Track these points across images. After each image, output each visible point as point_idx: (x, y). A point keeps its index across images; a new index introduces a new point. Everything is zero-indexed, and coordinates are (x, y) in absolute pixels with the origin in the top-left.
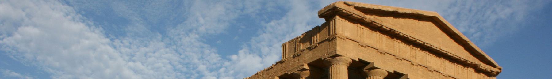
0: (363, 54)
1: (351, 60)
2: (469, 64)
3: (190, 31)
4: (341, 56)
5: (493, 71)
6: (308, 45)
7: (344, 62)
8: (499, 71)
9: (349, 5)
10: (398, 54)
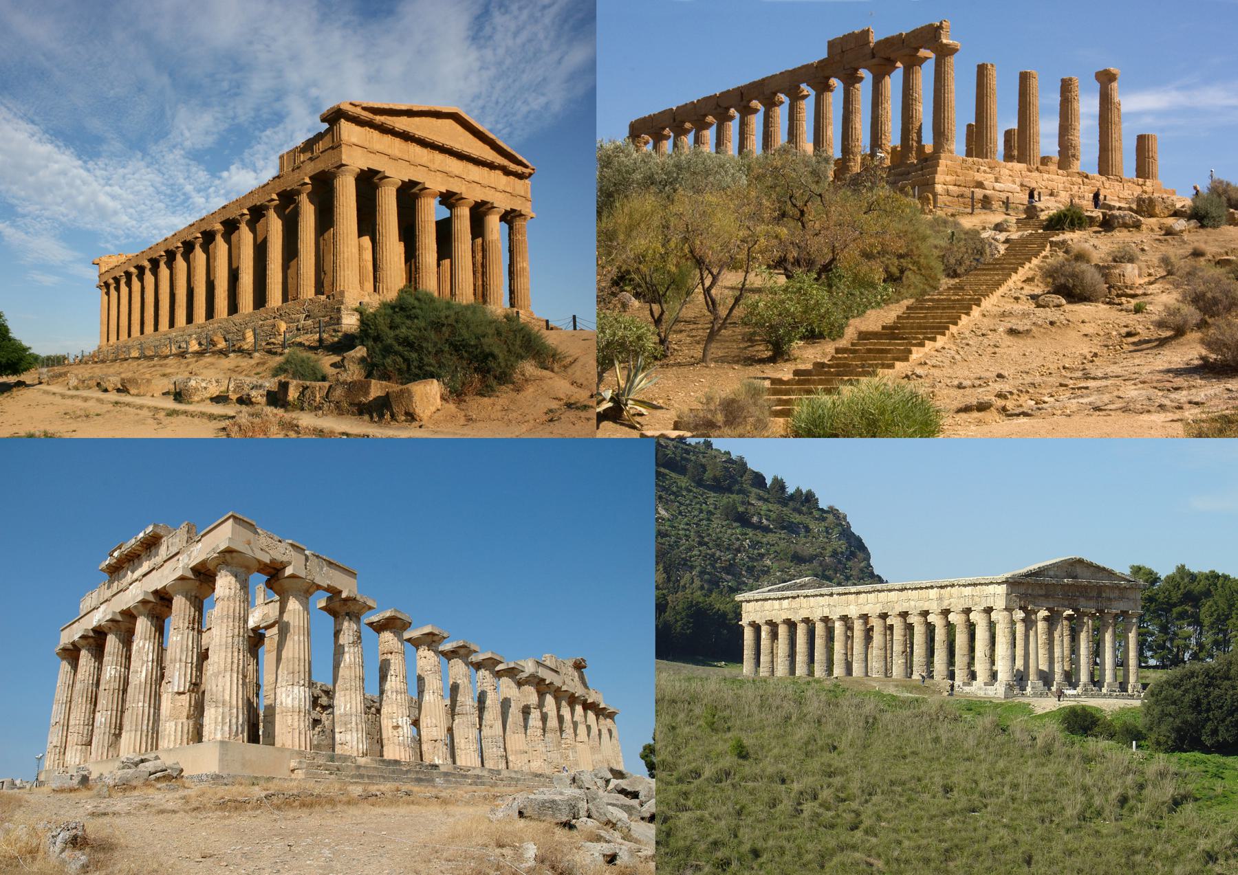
3: (174, 147)
6: (309, 155)
9: (355, 106)
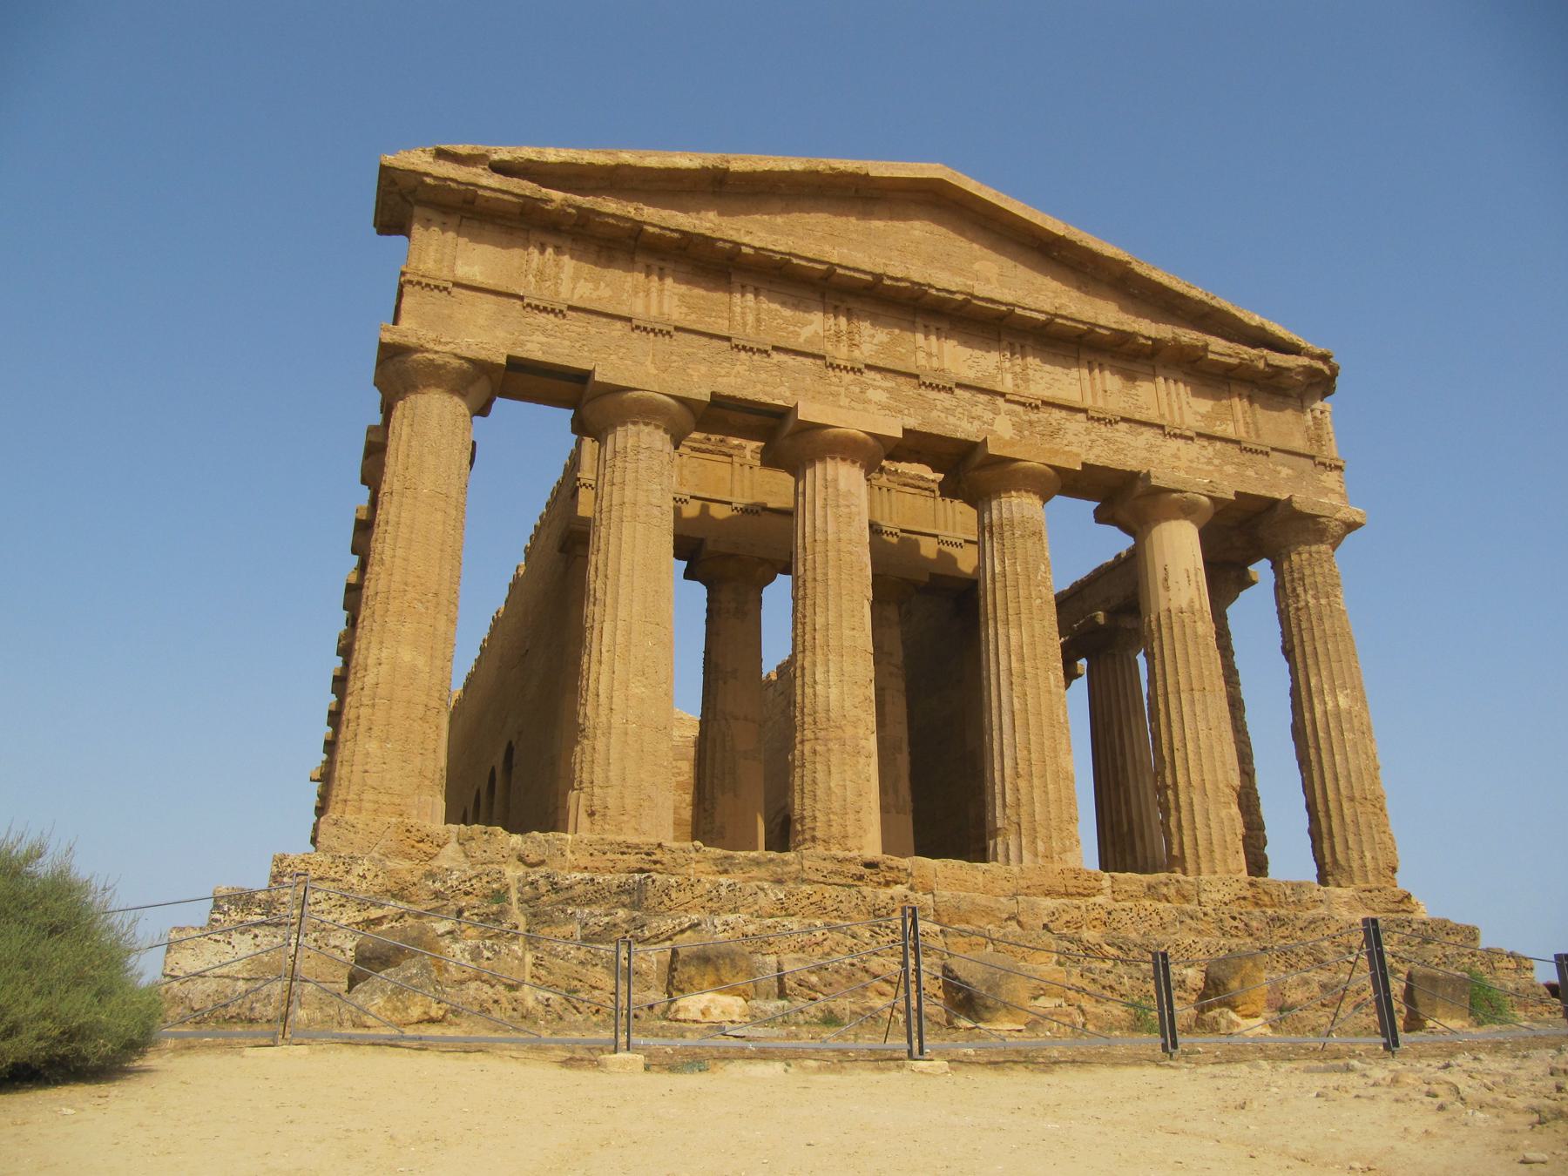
0: (543, 339)
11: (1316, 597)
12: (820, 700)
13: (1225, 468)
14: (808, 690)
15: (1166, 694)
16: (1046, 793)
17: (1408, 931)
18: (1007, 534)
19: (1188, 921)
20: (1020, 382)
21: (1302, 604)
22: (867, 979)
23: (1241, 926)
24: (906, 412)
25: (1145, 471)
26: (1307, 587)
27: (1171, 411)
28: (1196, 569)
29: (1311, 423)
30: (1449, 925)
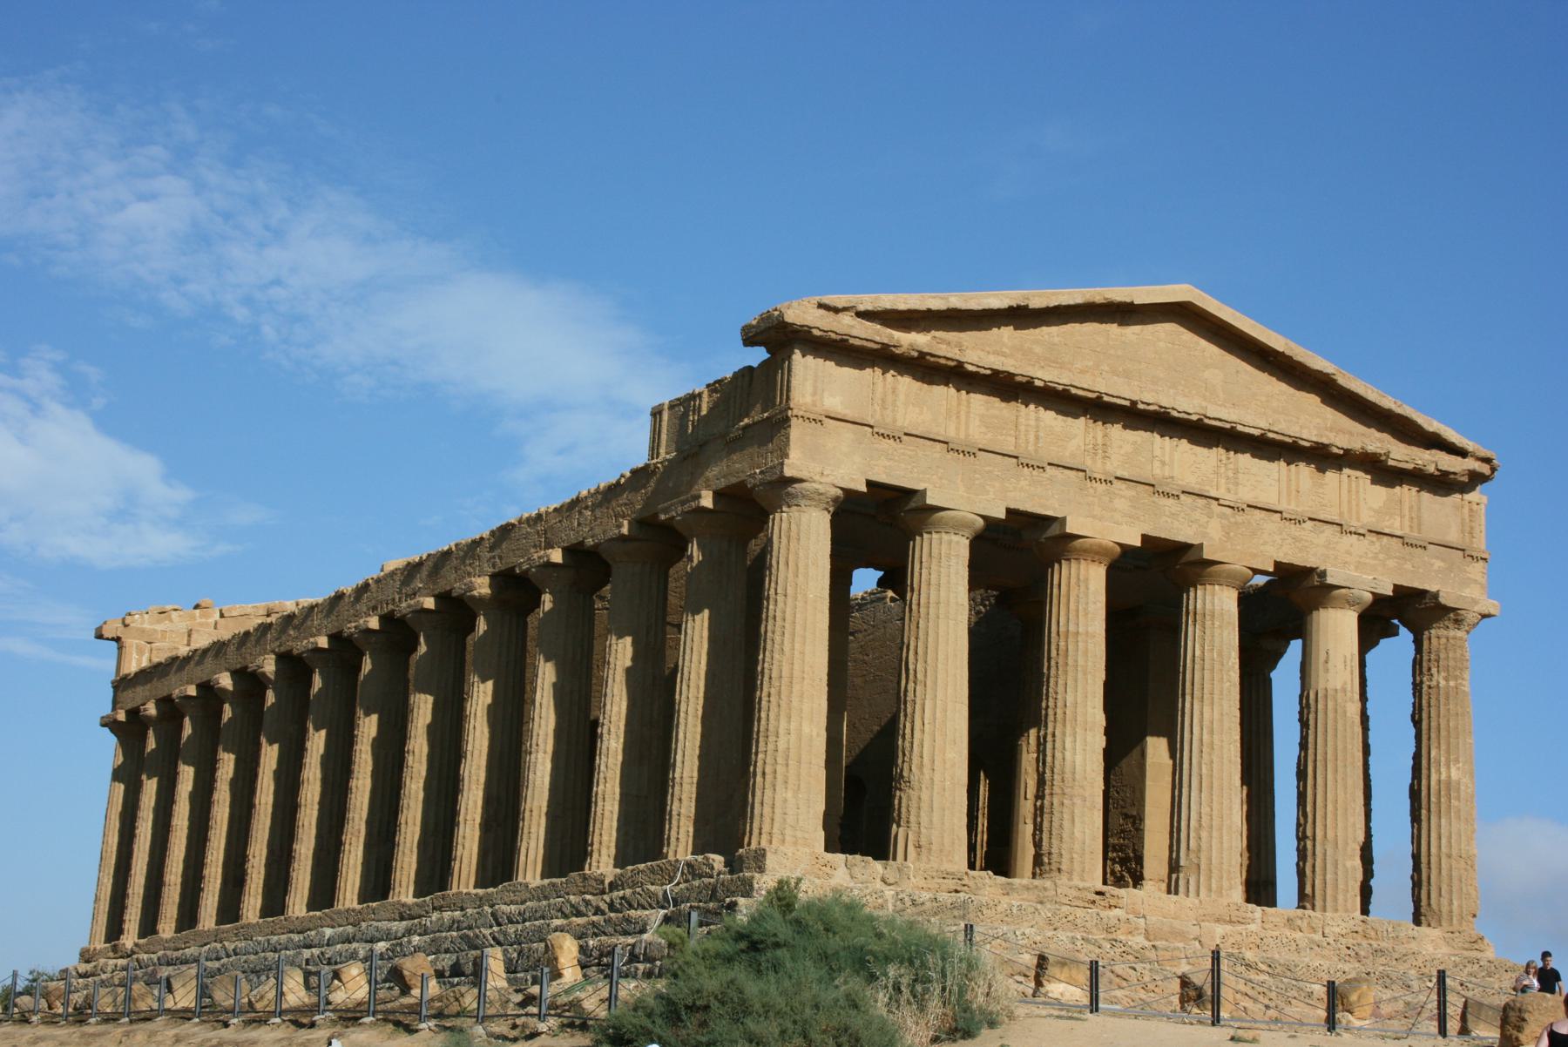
1: (840, 492)
2: (1337, 456)
4: (801, 481)
5: (1452, 470)
7: (811, 499)
8: (1485, 469)
10: (1031, 448)
11: (1446, 679)
12: (1068, 763)
13: (1387, 562)
14: (1058, 755)
15: (1315, 761)
16: (1222, 843)
17: (1476, 967)
18: (1208, 623)
19: (1316, 948)
20: (1231, 486)
21: (1434, 683)
22: (1112, 976)
23: (1353, 954)
24: (1142, 518)
25: (1322, 568)
26: (1441, 669)
27: (1350, 511)
28: (1352, 655)
29: (1467, 517)
30: (1508, 964)
